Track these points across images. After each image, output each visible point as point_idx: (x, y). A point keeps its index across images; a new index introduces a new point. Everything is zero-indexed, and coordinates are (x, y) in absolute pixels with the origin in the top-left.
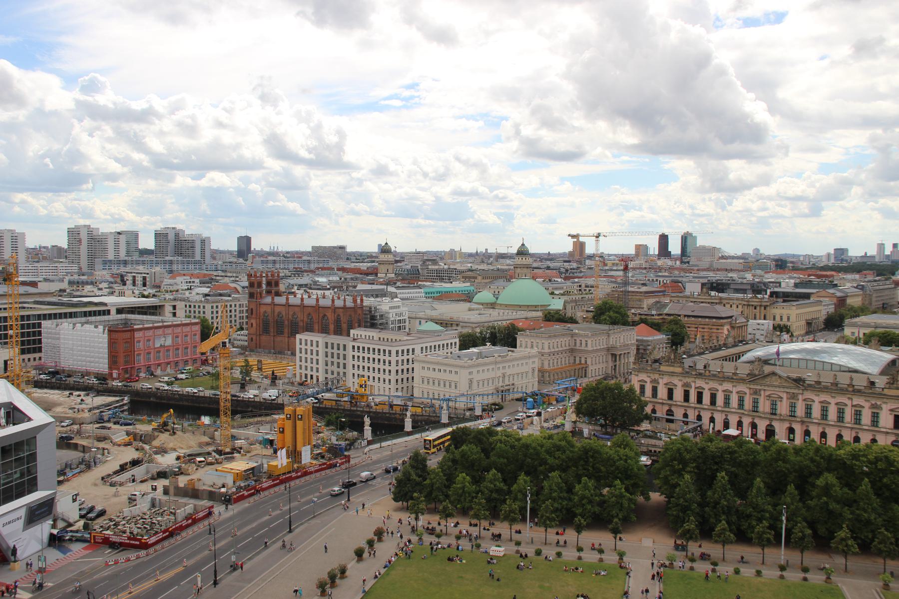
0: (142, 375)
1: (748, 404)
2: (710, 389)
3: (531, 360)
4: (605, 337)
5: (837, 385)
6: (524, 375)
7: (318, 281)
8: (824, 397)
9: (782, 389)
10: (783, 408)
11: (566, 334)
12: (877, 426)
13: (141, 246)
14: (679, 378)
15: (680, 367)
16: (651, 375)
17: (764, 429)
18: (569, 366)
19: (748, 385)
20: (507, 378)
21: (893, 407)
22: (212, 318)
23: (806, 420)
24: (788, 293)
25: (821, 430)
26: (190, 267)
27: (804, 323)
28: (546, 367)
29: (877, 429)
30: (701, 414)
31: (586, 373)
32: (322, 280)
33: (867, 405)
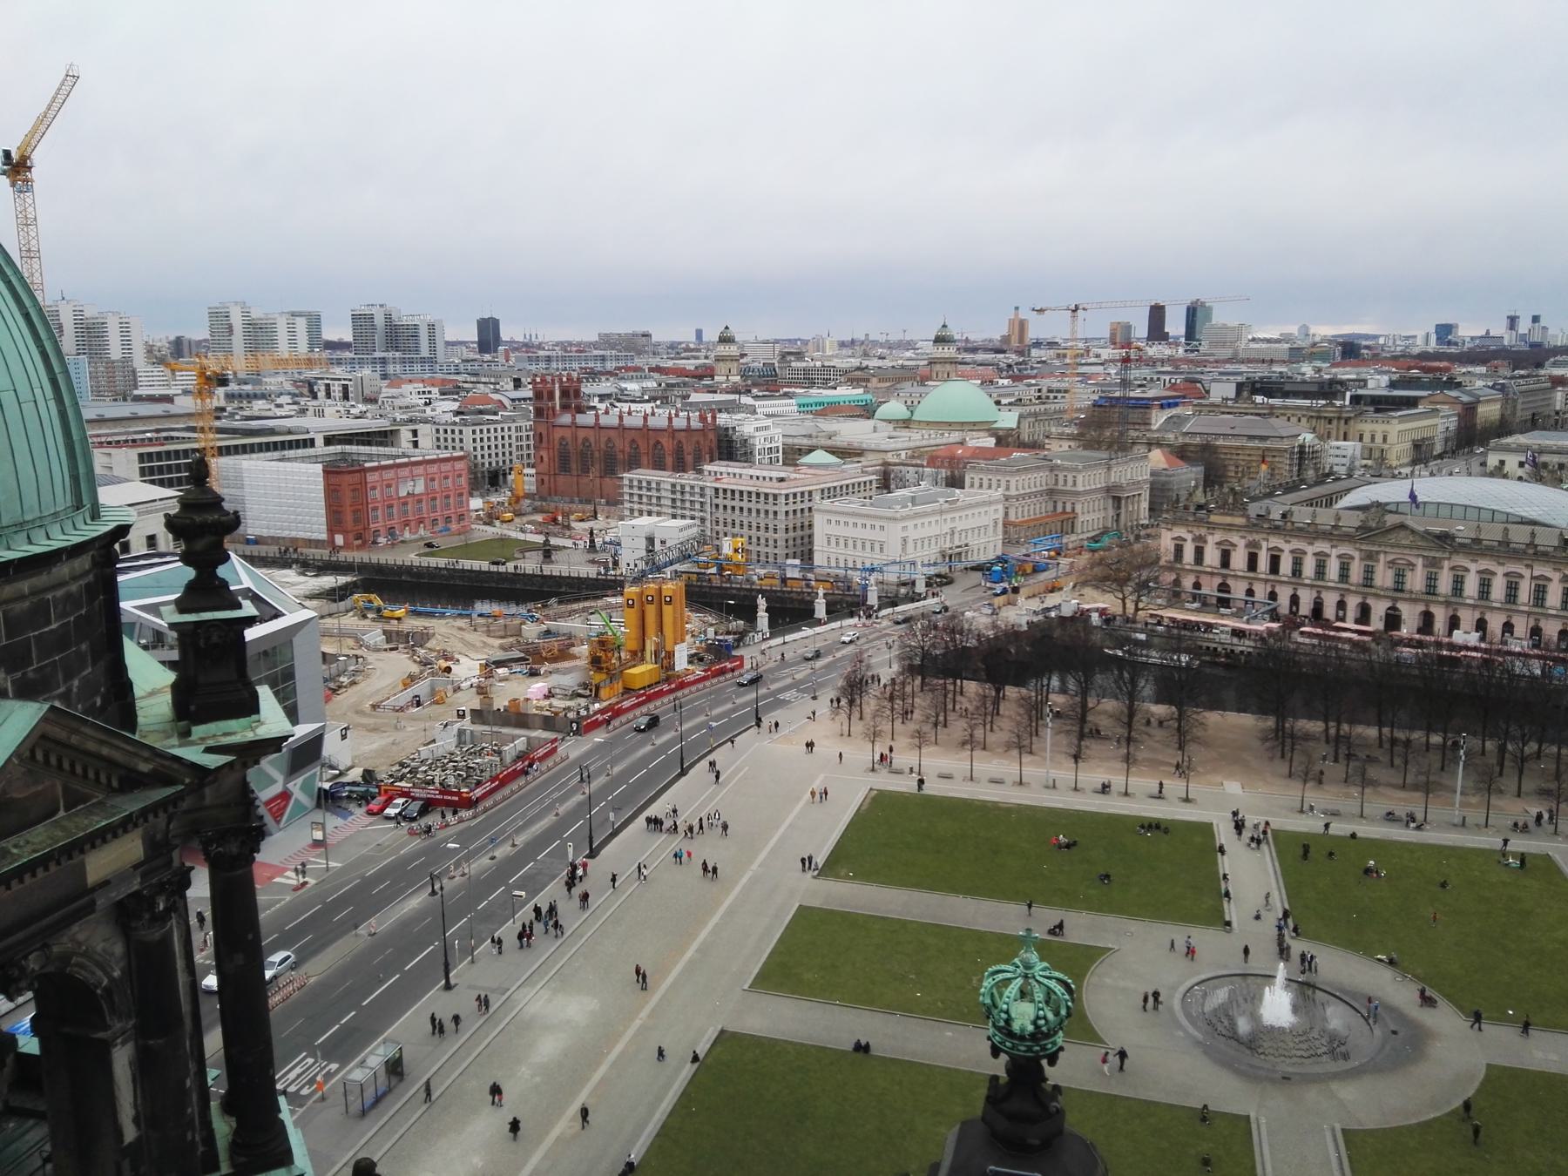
0: (382, 540)
2: (1292, 552)
3: (993, 508)
4: (1102, 471)
5: (1508, 544)
6: (983, 530)
7: (626, 389)
8: (1485, 564)
9: (1416, 552)
10: (1416, 581)
11: (1038, 467)
13: (329, 334)
14: (1240, 534)
15: (1242, 516)
16: (1195, 530)
17: (1383, 614)
18: (1048, 517)
19: (1358, 546)
22: (475, 449)
23: (1453, 599)
24: (1380, 397)
25: (1477, 615)
26: (415, 368)
27: (1409, 445)
28: (1012, 518)
31: (1073, 527)
32: (633, 387)
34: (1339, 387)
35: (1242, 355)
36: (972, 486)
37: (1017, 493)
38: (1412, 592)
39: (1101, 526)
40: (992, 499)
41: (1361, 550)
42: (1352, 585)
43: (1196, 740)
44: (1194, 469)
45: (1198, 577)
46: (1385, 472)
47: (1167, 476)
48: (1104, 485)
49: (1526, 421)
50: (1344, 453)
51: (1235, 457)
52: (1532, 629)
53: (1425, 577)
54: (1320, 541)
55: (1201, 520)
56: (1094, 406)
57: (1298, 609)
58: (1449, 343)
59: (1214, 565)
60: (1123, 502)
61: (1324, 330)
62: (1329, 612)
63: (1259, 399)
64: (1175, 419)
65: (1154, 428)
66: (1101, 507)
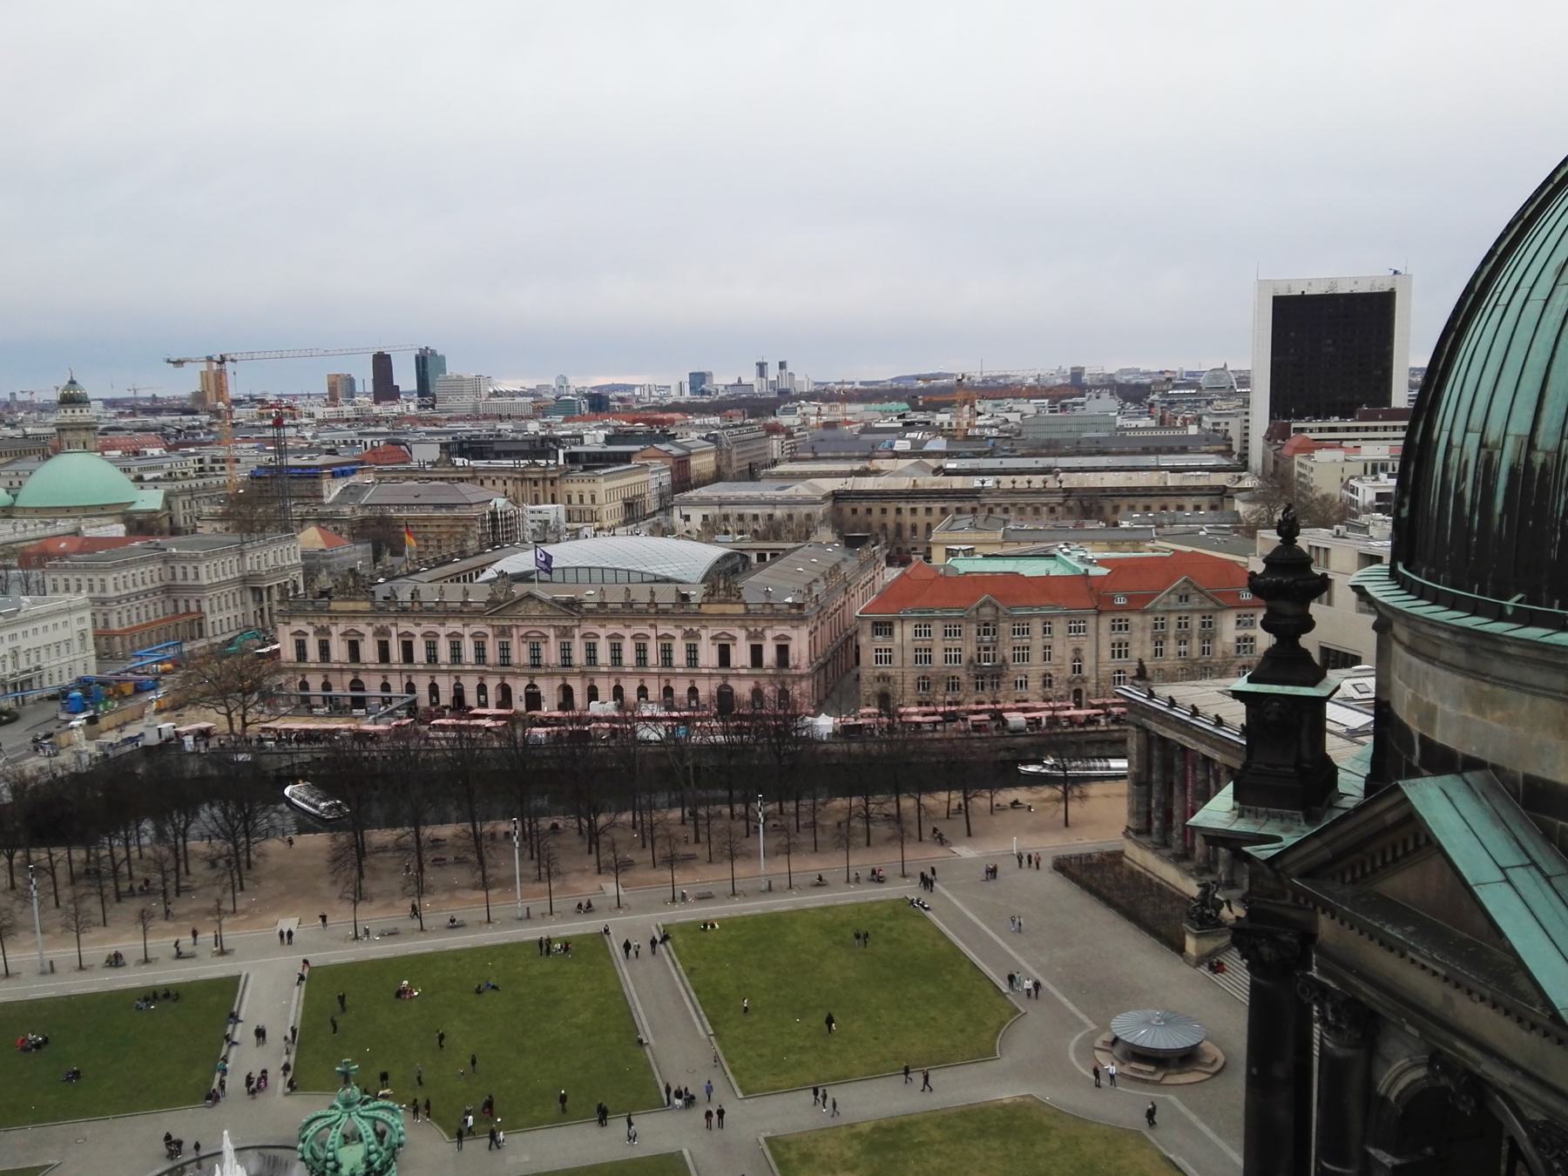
2: (424, 635)
4: (234, 558)
5: (631, 605)
8: (614, 628)
10: (551, 654)
12: (696, 666)
15: (366, 600)
16: (316, 621)
17: (523, 694)
19: (489, 621)
20: (22, 658)
21: (715, 633)
23: (588, 669)
29: (695, 671)
30: (414, 681)
33: (678, 633)
36: (55, 589)
37: (118, 594)
38: (548, 666)
40: (71, 605)
41: (493, 626)
42: (488, 666)
45: (326, 676)
51: (422, 529)
52: (665, 689)
53: (559, 649)
54: (451, 620)
56: (252, 478)
59: (342, 660)
62: (471, 698)
65: (327, 500)
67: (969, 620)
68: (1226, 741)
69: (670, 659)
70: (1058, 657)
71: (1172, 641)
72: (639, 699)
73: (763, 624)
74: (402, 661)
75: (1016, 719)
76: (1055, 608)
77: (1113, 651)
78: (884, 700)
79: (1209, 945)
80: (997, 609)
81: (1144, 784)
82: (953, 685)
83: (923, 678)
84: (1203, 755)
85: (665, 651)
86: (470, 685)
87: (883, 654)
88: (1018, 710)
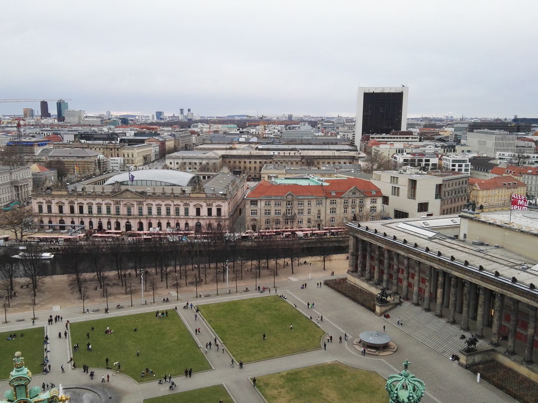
1: (113, 210)
9: (133, 200)
10: (135, 211)
12: (188, 215)
14: (65, 199)
15: (65, 191)
16: (46, 198)
19: (112, 199)
23: (149, 216)
25: (158, 221)
27: (142, 158)
33: (182, 204)
34: (115, 136)
35: (82, 123)
38: (134, 215)
39: (10, 200)
41: (113, 201)
42: (112, 215)
43: (40, 291)
44: (52, 172)
45: (50, 218)
46: (126, 169)
47: (40, 175)
48: (9, 181)
49: (183, 147)
50: (117, 162)
52: (176, 224)
54: (98, 198)
55: (48, 194)
57: (92, 227)
58: (161, 119)
59: (56, 213)
60: (19, 188)
61: (116, 113)
62: (105, 227)
63: (83, 141)
64: (45, 151)
66: (9, 191)
67: (283, 200)
68: (388, 241)
69: (179, 213)
70: (313, 213)
71: (350, 208)
72: (167, 228)
73: (212, 201)
74: (79, 213)
75: (300, 234)
76: (312, 196)
77: (331, 211)
78: (254, 228)
79: (384, 309)
80: (293, 196)
81: (355, 255)
82: (278, 222)
83: (268, 220)
84: (378, 246)
85: (177, 210)
86: (105, 222)
87: (254, 212)
88: (299, 231)
